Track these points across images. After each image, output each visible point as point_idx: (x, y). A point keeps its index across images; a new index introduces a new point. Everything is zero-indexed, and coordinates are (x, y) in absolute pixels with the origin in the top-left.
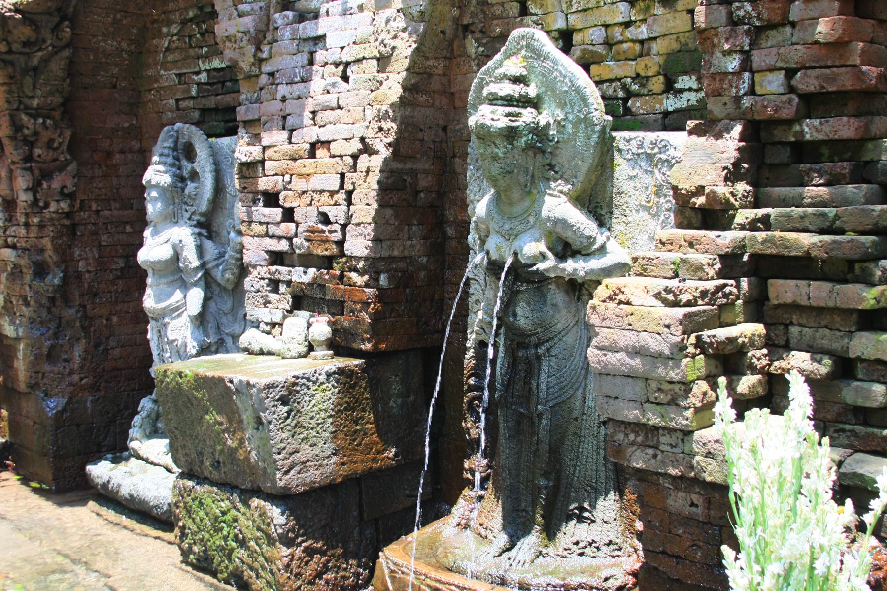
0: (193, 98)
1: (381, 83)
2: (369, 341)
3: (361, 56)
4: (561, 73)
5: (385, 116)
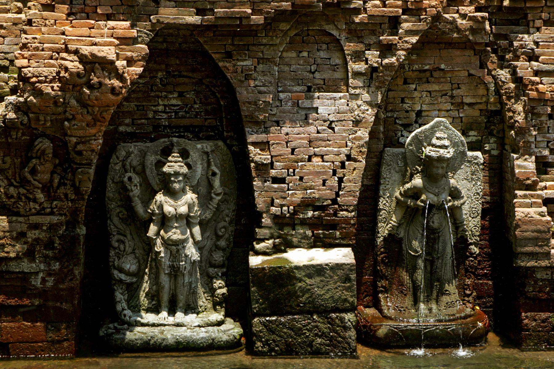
0: (148, 119)
1: (356, 132)
2: (354, 239)
3: (343, 119)
4: (455, 135)
5: (362, 146)
